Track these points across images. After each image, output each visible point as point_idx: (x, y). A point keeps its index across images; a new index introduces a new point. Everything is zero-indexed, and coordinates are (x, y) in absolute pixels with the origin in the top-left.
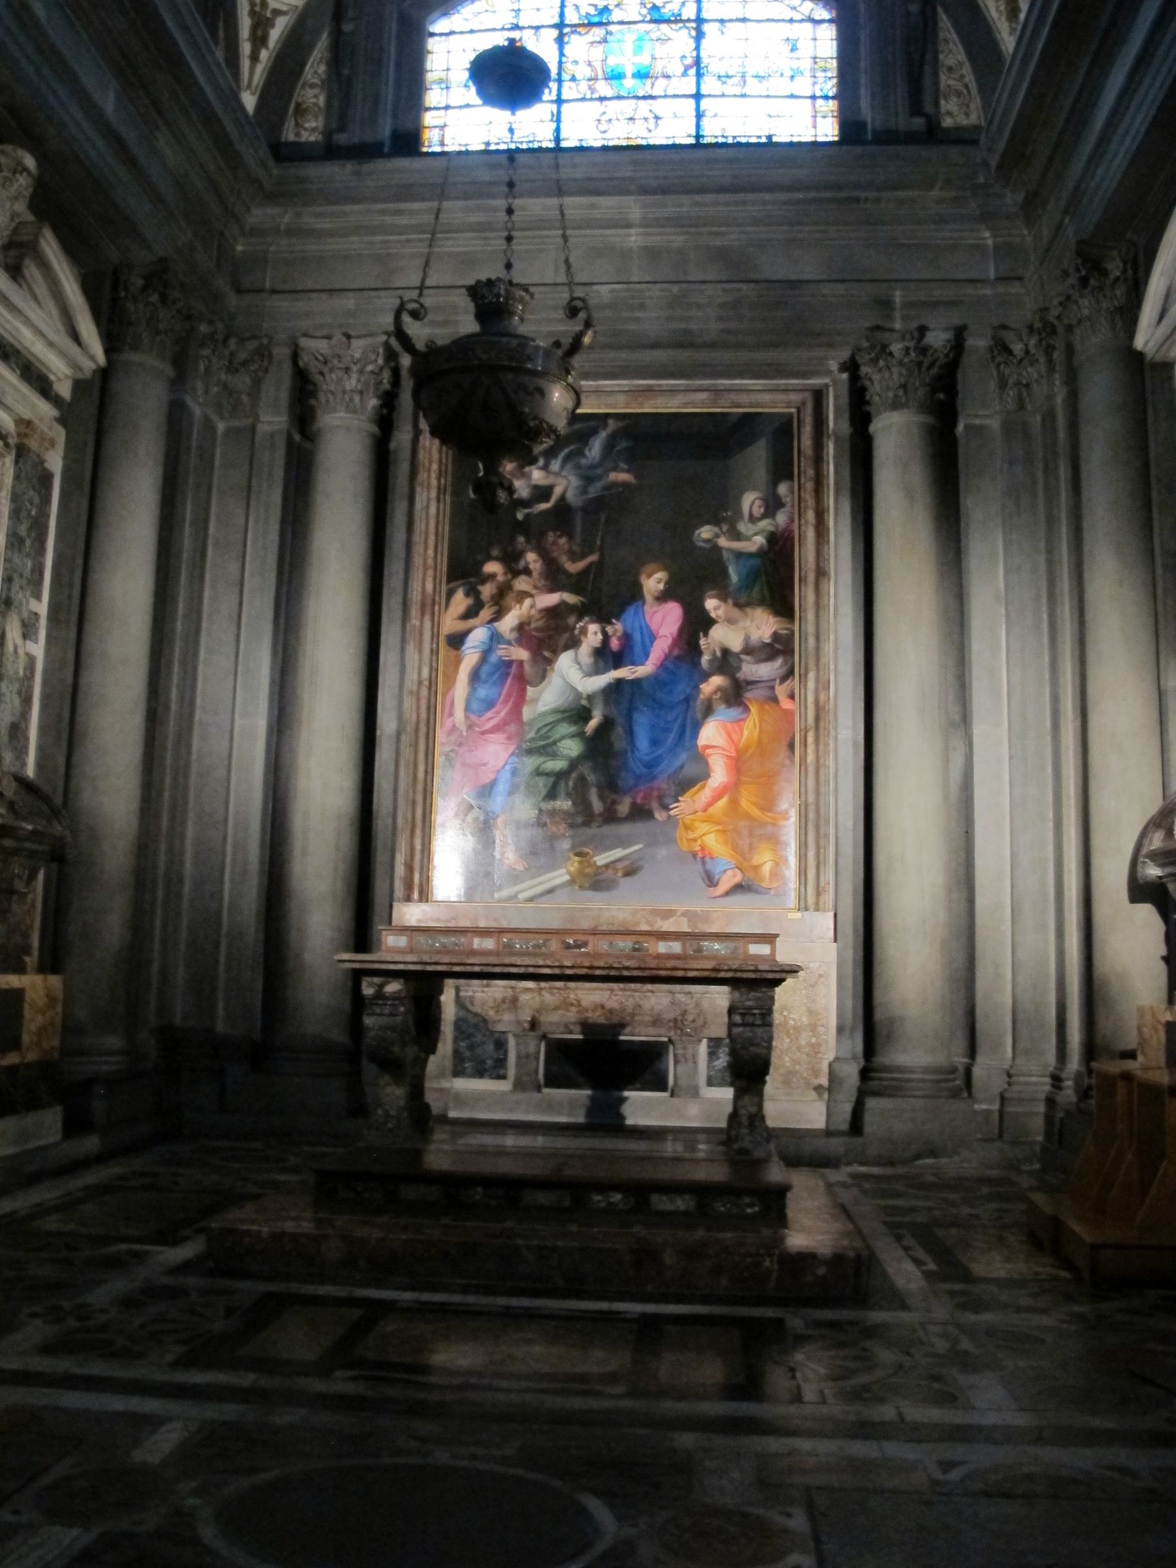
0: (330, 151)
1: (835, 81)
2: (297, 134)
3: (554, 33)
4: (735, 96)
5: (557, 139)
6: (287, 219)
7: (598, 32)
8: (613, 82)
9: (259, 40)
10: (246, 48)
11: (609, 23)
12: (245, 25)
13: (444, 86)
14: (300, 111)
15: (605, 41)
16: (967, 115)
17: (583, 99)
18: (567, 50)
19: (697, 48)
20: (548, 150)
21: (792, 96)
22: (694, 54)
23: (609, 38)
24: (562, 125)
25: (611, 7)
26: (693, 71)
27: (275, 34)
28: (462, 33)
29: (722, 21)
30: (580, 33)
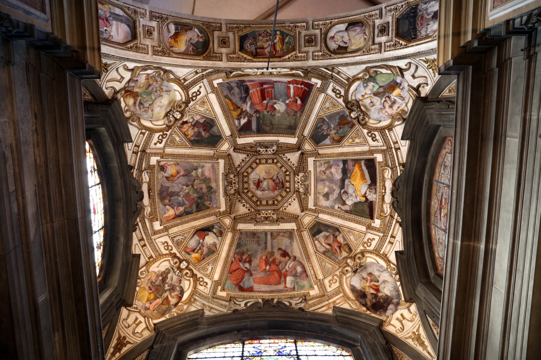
11: (261, 356)
12: (114, 342)
27: (125, 349)
29: (307, 355)
30: (250, 359)
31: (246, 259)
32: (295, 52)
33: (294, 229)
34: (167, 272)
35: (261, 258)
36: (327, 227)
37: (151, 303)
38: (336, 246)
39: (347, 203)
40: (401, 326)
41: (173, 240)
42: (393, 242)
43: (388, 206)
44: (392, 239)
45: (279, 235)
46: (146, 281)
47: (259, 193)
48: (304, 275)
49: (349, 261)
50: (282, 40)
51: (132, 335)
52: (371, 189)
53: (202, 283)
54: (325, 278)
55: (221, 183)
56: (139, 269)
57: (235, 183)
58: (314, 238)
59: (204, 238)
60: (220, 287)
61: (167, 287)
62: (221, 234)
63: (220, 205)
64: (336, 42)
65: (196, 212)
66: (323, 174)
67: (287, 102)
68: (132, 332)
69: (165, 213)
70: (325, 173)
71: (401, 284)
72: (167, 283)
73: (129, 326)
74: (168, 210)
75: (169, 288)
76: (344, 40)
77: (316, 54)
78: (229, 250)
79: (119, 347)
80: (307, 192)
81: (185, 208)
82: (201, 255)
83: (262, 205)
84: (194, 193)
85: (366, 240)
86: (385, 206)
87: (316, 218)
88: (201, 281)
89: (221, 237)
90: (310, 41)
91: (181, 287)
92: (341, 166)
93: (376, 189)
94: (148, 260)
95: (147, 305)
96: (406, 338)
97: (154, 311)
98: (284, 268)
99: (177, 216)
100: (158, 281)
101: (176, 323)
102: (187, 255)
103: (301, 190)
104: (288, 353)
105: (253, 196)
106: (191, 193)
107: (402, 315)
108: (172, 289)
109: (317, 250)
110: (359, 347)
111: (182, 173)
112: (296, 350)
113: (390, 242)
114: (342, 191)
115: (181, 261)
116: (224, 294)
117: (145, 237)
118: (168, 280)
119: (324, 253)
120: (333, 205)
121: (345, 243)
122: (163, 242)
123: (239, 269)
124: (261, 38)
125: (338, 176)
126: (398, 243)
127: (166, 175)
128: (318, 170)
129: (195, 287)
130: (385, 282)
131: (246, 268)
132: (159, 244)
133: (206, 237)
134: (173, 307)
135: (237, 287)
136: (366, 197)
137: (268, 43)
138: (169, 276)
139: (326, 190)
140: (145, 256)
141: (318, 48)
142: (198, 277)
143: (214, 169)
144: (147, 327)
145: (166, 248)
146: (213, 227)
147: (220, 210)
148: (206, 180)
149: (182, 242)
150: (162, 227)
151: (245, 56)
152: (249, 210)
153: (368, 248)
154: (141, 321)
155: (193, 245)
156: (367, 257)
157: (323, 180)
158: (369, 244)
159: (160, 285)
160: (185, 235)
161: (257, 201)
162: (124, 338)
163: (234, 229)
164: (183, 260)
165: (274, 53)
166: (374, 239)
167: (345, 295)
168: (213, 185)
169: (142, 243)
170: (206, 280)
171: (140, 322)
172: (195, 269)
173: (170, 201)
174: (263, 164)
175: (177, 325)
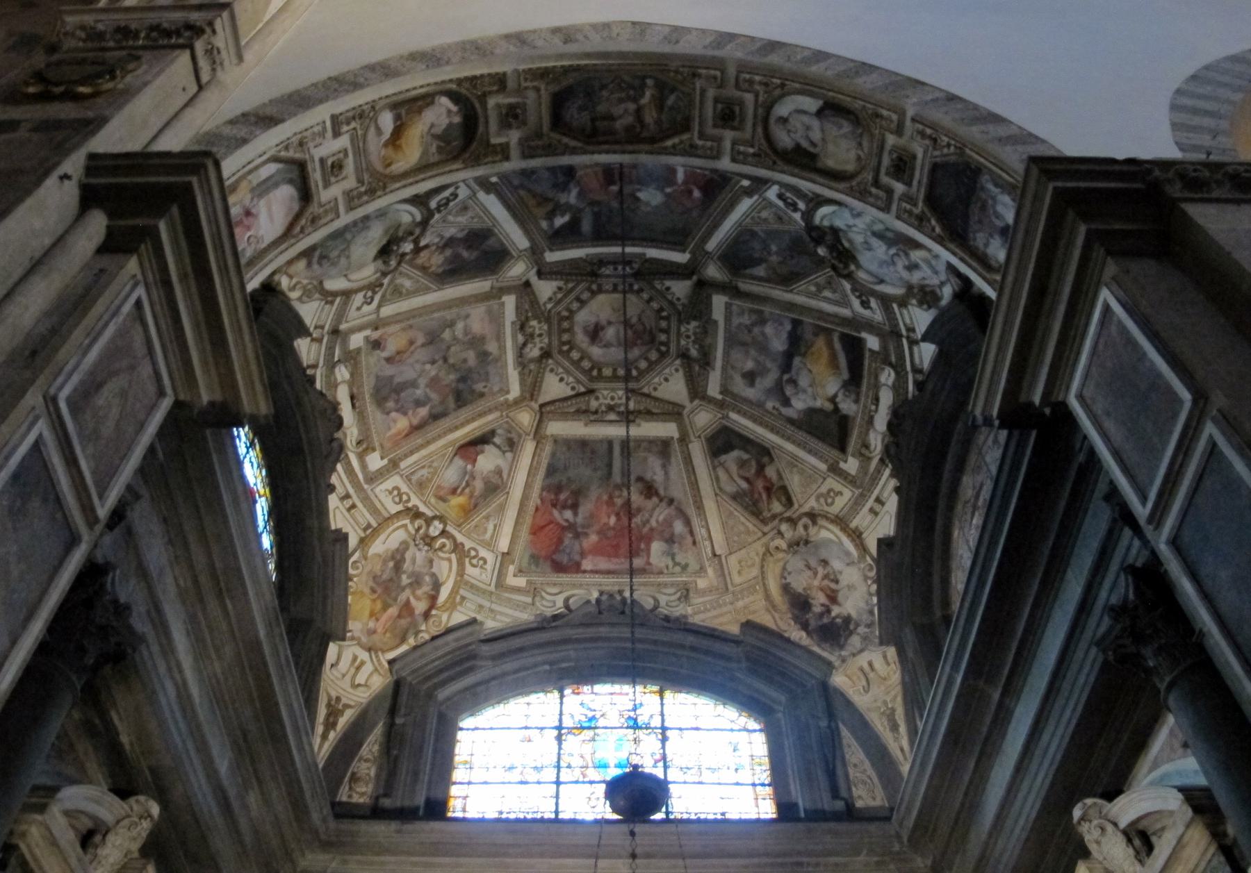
0: (376, 812)
1: (769, 772)
2: (350, 796)
3: (555, 733)
4: (694, 783)
5: (557, 812)
6: (334, 865)
7: (588, 734)
8: (600, 770)
9: (330, 725)
10: (320, 729)
11: (596, 728)
13: (468, 766)
14: (354, 779)
15: (593, 740)
16: (874, 799)
17: (577, 782)
18: (564, 745)
19: (663, 747)
20: (550, 821)
21: (737, 784)
22: (661, 751)
23: (597, 738)
24: (560, 801)
25: (597, 716)
26: (661, 764)
27: (343, 722)
28: (484, 729)
29: (680, 729)
30: (574, 734)
31: (566, 500)
32: (685, 137)
33: (672, 438)
34: (404, 546)
35: (599, 498)
36: (746, 442)
37: (377, 620)
38: (760, 485)
39: (794, 402)
40: (864, 683)
41: (410, 480)
42: (878, 510)
43: (879, 438)
44: (877, 507)
45: (639, 446)
46: (364, 578)
47: (596, 351)
48: (689, 539)
49: (784, 527)
50: (660, 103)
51: (350, 690)
52: (849, 391)
53: (474, 561)
54: (730, 554)
55: (509, 344)
56: (349, 556)
57: (540, 335)
58: (716, 463)
59: (475, 461)
60: (512, 569)
61: (405, 580)
62: (512, 445)
63: (508, 387)
64: (792, 135)
65: (455, 410)
66: (746, 332)
67: (668, 190)
68: (349, 684)
69: (389, 429)
70: (750, 331)
71: (879, 601)
72: (404, 572)
73: (344, 676)
74: (395, 421)
75: (409, 581)
76: (811, 134)
77: (742, 148)
78: (528, 486)
79: (331, 720)
80: (706, 361)
81: (432, 408)
82: (471, 496)
83: (602, 378)
84: (449, 374)
85: (824, 489)
86: (872, 436)
87: (723, 418)
88: (474, 557)
89: (511, 451)
90: (728, 115)
91: (433, 575)
92: (788, 327)
93: (858, 394)
94: (363, 535)
95: (371, 625)
96: (869, 710)
97: (385, 633)
98: (648, 521)
99: (416, 429)
100: (388, 571)
101: (429, 659)
102: (441, 503)
103: (694, 352)
104: (646, 721)
105: (582, 358)
106: (442, 374)
107: (870, 664)
108: (417, 582)
109: (720, 489)
110: (780, 715)
111: (421, 340)
112: (662, 715)
113: (872, 510)
114: (786, 377)
115: (429, 521)
116: (521, 582)
117: (351, 491)
118: (407, 566)
119: (735, 497)
120: (763, 398)
121: (781, 484)
122: (390, 488)
123: (551, 522)
124: (605, 93)
125: (779, 344)
126: (887, 518)
127: (385, 354)
128: (736, 321)
129: (461, 572)
130: (851, 587)
131: (567, 521)
132: (382, 497)
133: (479, 457)
134: (420, 619)
135: (549, 563)
136: (835, 404)
137: (623, 106)
138: (408, 555)
139: (750, 365)
140: (357, 528)
141: (747, 134)
142: (467, 548)
143: (496, 318)
144: (376, 670)
145: (397, 499)
146: (493, 433)
147: (508, 396)
148: (476, 342)
149: (429, 480)
150: (385, 461)
151: (565, 140)
152: (573, 388)
153: (826, 508)
154: (365, 659)
155: (452, 481)
156: (822, 527)
157: (744, 344)
158: (830, 501)
159: (391, 580)
160: (435, 464)
161: (592, 369)
162: (338, 699)
163: (538, 435)
164: (434, 518)
165: (638, 130)
166: (840, 493)
167: (768, 596)
168: (492, 347)
169: (348, 503)
170: (483, 553)
171: (363, 663)
172: (460, 532)
173: (397, 401)
174: (607, 292)
175: (433, 661)
